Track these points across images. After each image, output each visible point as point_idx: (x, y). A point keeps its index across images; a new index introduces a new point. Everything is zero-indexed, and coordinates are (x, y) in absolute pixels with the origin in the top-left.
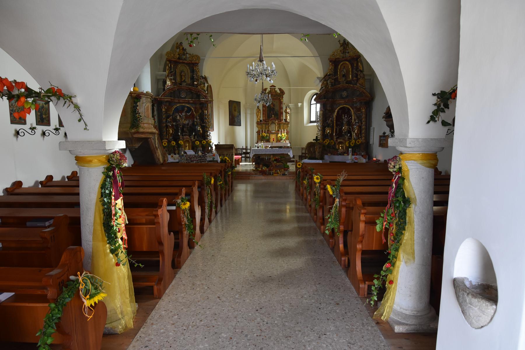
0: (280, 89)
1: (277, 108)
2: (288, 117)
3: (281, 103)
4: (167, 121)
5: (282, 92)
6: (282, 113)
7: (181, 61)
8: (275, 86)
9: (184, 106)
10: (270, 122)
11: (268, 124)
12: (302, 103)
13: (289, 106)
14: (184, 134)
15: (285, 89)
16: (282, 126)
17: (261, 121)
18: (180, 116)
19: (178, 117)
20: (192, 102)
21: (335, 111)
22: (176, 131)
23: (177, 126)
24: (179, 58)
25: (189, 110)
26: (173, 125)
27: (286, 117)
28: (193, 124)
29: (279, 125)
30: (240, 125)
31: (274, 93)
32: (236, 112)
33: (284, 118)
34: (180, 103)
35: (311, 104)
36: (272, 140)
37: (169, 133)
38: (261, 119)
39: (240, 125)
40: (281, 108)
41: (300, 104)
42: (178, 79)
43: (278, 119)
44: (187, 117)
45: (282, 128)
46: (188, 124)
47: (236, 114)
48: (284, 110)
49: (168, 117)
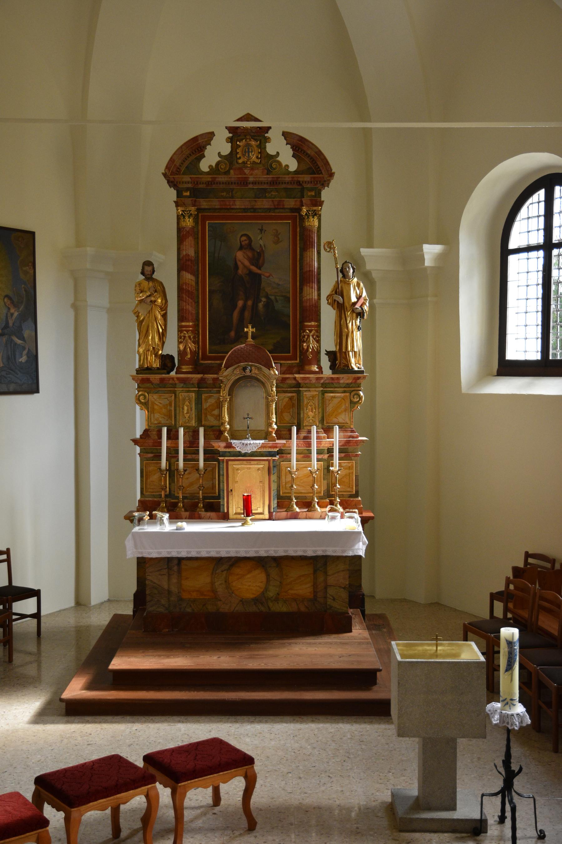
1: (277, 277)
2: (357, 341)
3: (304, 240)
5: (315, 167)
6: (314, 313)
10: (228, 375)
11: (217, 385)
12: (449, 239)
13: (358, 264)
15: (330, 137)
16: (310, 395)
17: (167, 362)
27: (342, 335)
29: (293, 390)
30: (32, 387)
31: (259, 175)
33: (328, 342)
35: (506, 252)
36: (235, 506)
38: (171, 348)
40: (307, 277)
41: (431, 251)
45: (310, 414)
48: (327, 284)
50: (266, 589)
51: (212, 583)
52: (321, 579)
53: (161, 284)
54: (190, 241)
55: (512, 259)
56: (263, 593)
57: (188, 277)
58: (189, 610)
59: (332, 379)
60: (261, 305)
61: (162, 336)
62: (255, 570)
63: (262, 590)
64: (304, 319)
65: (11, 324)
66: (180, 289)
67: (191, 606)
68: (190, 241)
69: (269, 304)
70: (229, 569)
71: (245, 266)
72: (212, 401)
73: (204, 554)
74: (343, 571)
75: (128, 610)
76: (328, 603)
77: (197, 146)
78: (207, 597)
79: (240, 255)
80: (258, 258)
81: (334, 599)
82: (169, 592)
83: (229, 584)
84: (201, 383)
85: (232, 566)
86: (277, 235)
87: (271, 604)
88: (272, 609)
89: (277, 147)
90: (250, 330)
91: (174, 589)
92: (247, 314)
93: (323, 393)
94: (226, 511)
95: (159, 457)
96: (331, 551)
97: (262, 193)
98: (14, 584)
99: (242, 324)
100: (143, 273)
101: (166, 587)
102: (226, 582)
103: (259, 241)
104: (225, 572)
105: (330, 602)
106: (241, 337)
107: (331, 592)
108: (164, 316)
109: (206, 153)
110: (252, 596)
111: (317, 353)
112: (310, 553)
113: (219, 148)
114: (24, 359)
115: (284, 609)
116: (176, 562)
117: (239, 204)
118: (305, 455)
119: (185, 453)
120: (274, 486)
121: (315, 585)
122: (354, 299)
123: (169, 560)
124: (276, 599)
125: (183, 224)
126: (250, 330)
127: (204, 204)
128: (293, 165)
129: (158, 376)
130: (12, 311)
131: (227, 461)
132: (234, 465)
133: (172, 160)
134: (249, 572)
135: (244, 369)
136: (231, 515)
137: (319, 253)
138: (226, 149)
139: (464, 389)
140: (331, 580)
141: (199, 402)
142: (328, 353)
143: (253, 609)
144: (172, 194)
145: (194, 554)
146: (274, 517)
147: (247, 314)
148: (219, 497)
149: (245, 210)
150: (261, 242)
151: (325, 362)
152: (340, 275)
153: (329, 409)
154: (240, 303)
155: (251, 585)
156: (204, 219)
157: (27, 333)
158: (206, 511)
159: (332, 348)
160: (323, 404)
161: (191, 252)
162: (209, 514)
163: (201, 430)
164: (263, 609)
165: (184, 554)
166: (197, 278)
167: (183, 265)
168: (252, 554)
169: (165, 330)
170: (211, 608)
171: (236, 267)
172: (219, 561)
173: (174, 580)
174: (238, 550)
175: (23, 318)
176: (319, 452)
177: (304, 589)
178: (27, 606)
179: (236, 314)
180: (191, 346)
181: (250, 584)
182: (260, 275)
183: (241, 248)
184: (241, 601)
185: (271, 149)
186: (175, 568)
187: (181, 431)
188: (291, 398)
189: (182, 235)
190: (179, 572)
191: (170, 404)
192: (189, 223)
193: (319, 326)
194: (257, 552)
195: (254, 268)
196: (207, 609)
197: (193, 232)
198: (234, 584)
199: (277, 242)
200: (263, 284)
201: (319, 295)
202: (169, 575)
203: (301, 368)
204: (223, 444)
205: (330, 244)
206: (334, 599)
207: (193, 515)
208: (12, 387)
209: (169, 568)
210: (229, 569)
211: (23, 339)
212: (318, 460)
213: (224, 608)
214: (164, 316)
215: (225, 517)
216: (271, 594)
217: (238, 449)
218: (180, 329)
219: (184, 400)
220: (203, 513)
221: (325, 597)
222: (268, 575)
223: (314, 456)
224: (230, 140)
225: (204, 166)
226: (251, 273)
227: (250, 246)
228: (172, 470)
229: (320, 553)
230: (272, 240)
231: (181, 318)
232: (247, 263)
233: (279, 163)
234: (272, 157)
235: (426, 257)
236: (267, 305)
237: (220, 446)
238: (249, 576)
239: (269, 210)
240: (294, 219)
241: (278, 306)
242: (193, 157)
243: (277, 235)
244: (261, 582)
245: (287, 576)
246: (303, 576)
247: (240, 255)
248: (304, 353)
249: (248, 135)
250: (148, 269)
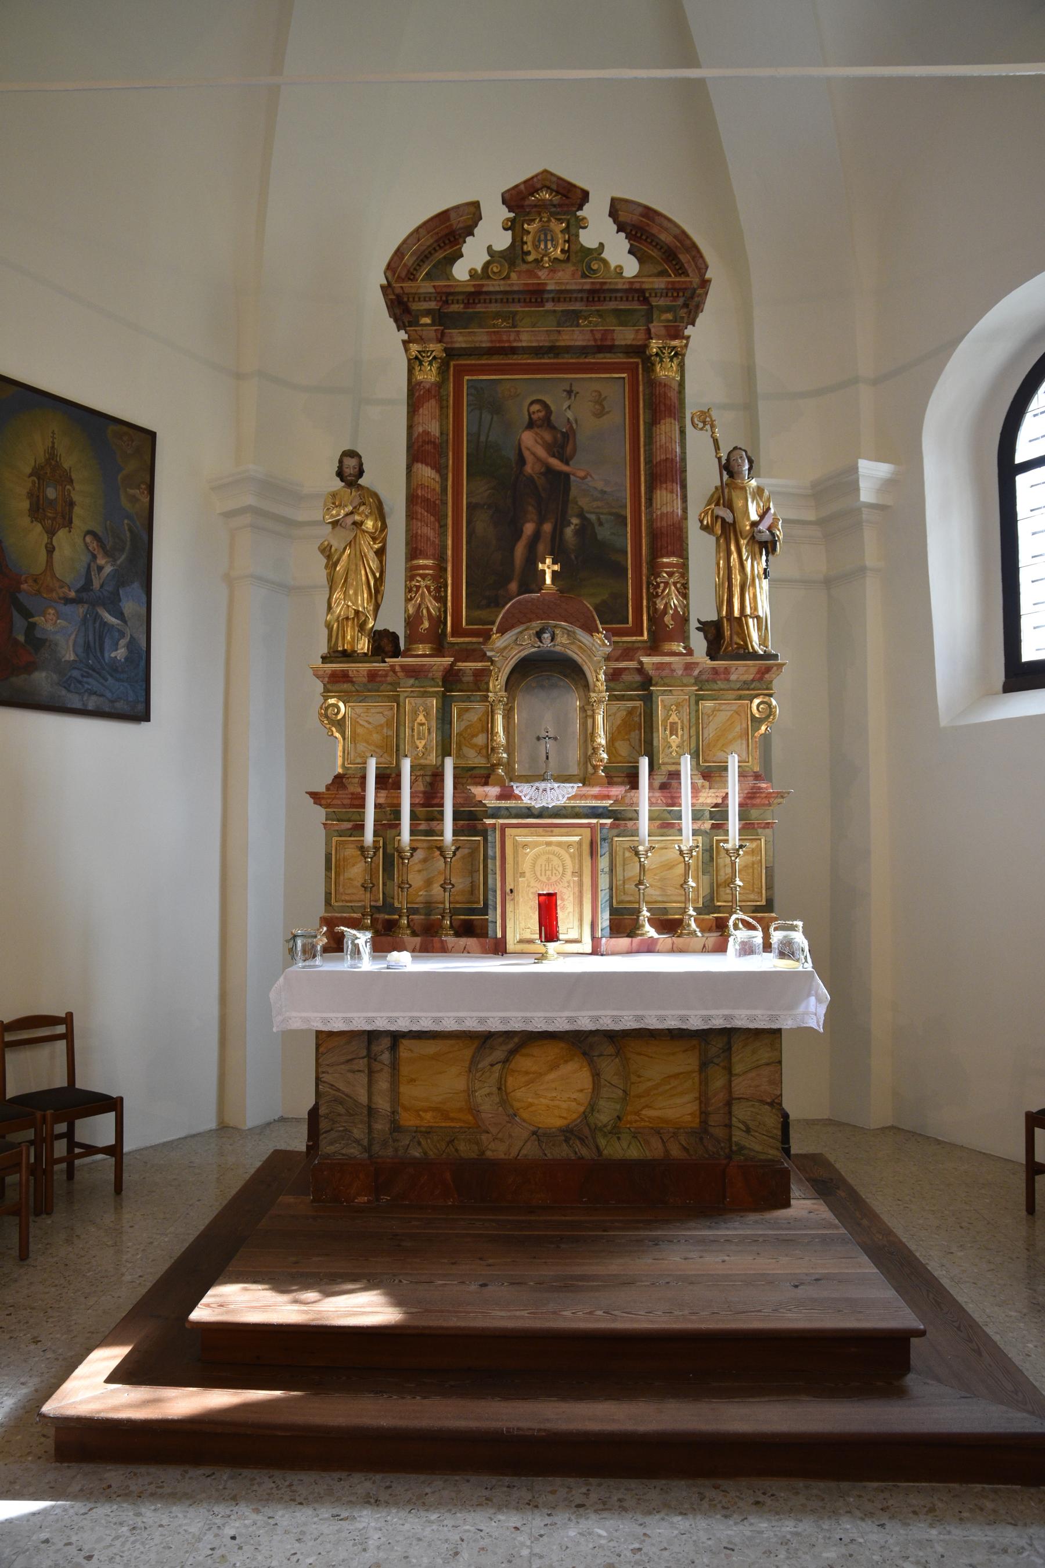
0: (638, 225)
1: (601, 476)
11: (481, 678)
12: (906, 453)
16: (669, 707)
17: (384, 644)
29: (639, 690)
30: (138, 712)
31: (566, 278)
32: (70, 550)
35: (1008, 470)
36: (521, 922)
38: (392, 618)
41: (872, 474)
43: (612, 615)
45: (670, 741)
50: (592, 1107)
51: (470, 1092)
52: (718, 1083)
53: (375, 495)
54: (429, 408)
55: (1022, 481)
56: (585, 1116)
57: (426, 473)
58: (417, 1153)
59: (715, 671)
60: (569, 532)
61: (376, 594)
62: (566, 1062)
63: (582, 1109)
64: (655, 553)
65: (96, 584)
66: (412, 499)
67: (419, 1143)
68: (429, 408)
69: (585, 530)
70: (506, 1061)
71: (538, 459)
72: (473, 717)
73: (449, 1025)
74: (767, 1064)
75: (299, 1143)
76: (734, 1139)
77: (449, 230)
78: (458, 1125)
79: (528, 438)
80: (563, 444)
81: (748, 1130)
82: (371, 1111)
83: (507, 1094)
84: (451, 679)
85: (513, 1052)
87: (602, 1142)
88: (605, 1152)
89: (599, 231)
90: (548, 568)
91: (383, 1104)
93: (699, 698)
94: (499, 935)
95: (360, 828)
96: (744, 1017)
97: (572, 318)
98: (78, 1085)
99: (532, 559)
100: (340, 474)
101: (363, 1099)
102: (499, 1089)
103: (564, 411)
104: (499, 1066)
105: (738, 1136)
106: (532, 579)
107: (741, 1112)
108: (380, 553)
109: (465, 249)
110: (560, 1123)
111: (683, 620)
112: (695, 1023)
113: (492, 235)
114: (120, 653)
115: (634, 1152)
116: (386, 1042)
117: (526, 339)
118: (666, 823)
119: (414, 816)
120: (604, 882)
121: (703, 1099)
122: (754, 517)
123: (372, 1036)
124: (614, 1131)
125: (420, 377)
127: (460, 339)
128: (631, 267)
129: (364, 667)
130: (101, 561)
131: (503, 827)
132: (517, 837)
133: (399, 253)
134: (554, 1067)
135: (539, 635)
136: (511, 946)
137: (683, 432)
138: (503, 241)
139: (944, 721)
140: (740, 1087)
141: (444, 718)
142: (704, 627)
143: (563, 1152)
145: (426, 1024)
146: (603, 949)
148: (484, 911)
149: (537, 351)
150: (569, 414)
151: (699, 642)
152: (726, 477)
153: (709, 732)
154: (529, 528)
155: (555, 1097)
156: (460, 371)
157: (129, 606)
158: (458, 934)
160: (696, 723)
161: (434, 428)
162: (463, 941)
163: (449, 763)
164: (584, 1152)
165: (403, 1025)
166: (444, 479)
167: (419, 451)
168: (561, 1025)
169: (380, 581)
170: (466, 1150)
171: (521, 460)
172: (484, 1040)
173: (383, 1084)
174: (528, 1014)
175: (121, 580)
176: (697, 816)
177: (678, 1107)
178: (98, 1130)
179: (520, 550)
180: (432, 605)
181: (554, 1094)
182: (567, 476)
183: (531, 425)
184: (534, 1133)
185: (588, 239)
186: (386, 1057)
187: (406, 765)
188: (631, 712)
189: (416, 396)
190: (395, 1066)
191: (389, 724)
192: (429, 375)
193: (684, 567)
194: (571, 1020)
195: (555, 463)
196: (457, 1150)
197: (436, 392)
198: (518, 1094)
199: (600, 414)
200: (574, 492)
201: (685, 510)
202: (371, 1073)
203: (654, 647)
204: (493, 791)
205: (705, 419)
206: (748, 1130)
207: (429, 938)
208: (92, 703)
209: (371, 1058)
210: (506, 1061)
211: (121, 616)
212: (695, 833)
213: (497, 1151)
214: (380, 553)
215: (499, 948)
216: (604, 1117)
217: (526, 800)
218: (411, 573)
219: (415, 713)
220: (450, 940)
221: (729, 1126)
222: (596, 1075)
223: (687, 823)
224: (510, 226)
225: (461, 271)
226: (549, 471)
227: (547, 421)
228: (390, 857)
229: (718, 1023)
230: (593, 408)
231: (413, 552)
232: (541, 452)
233: (605, 262)
234: (589, 251)
235: (863, 484)
236: (580, 532)
237: (488, 794)
238: (552, 1076)
239: (584, 351)
240: (632, 370)
241: (604, 533)
242: (440, 255)
243: (600, 401)
244: (581, 1091)
245: (639, 1076)
246: (676, 1076)
247: (528, 438)
248: (656, 619)
249: (546, 201)
250: (350, 463)
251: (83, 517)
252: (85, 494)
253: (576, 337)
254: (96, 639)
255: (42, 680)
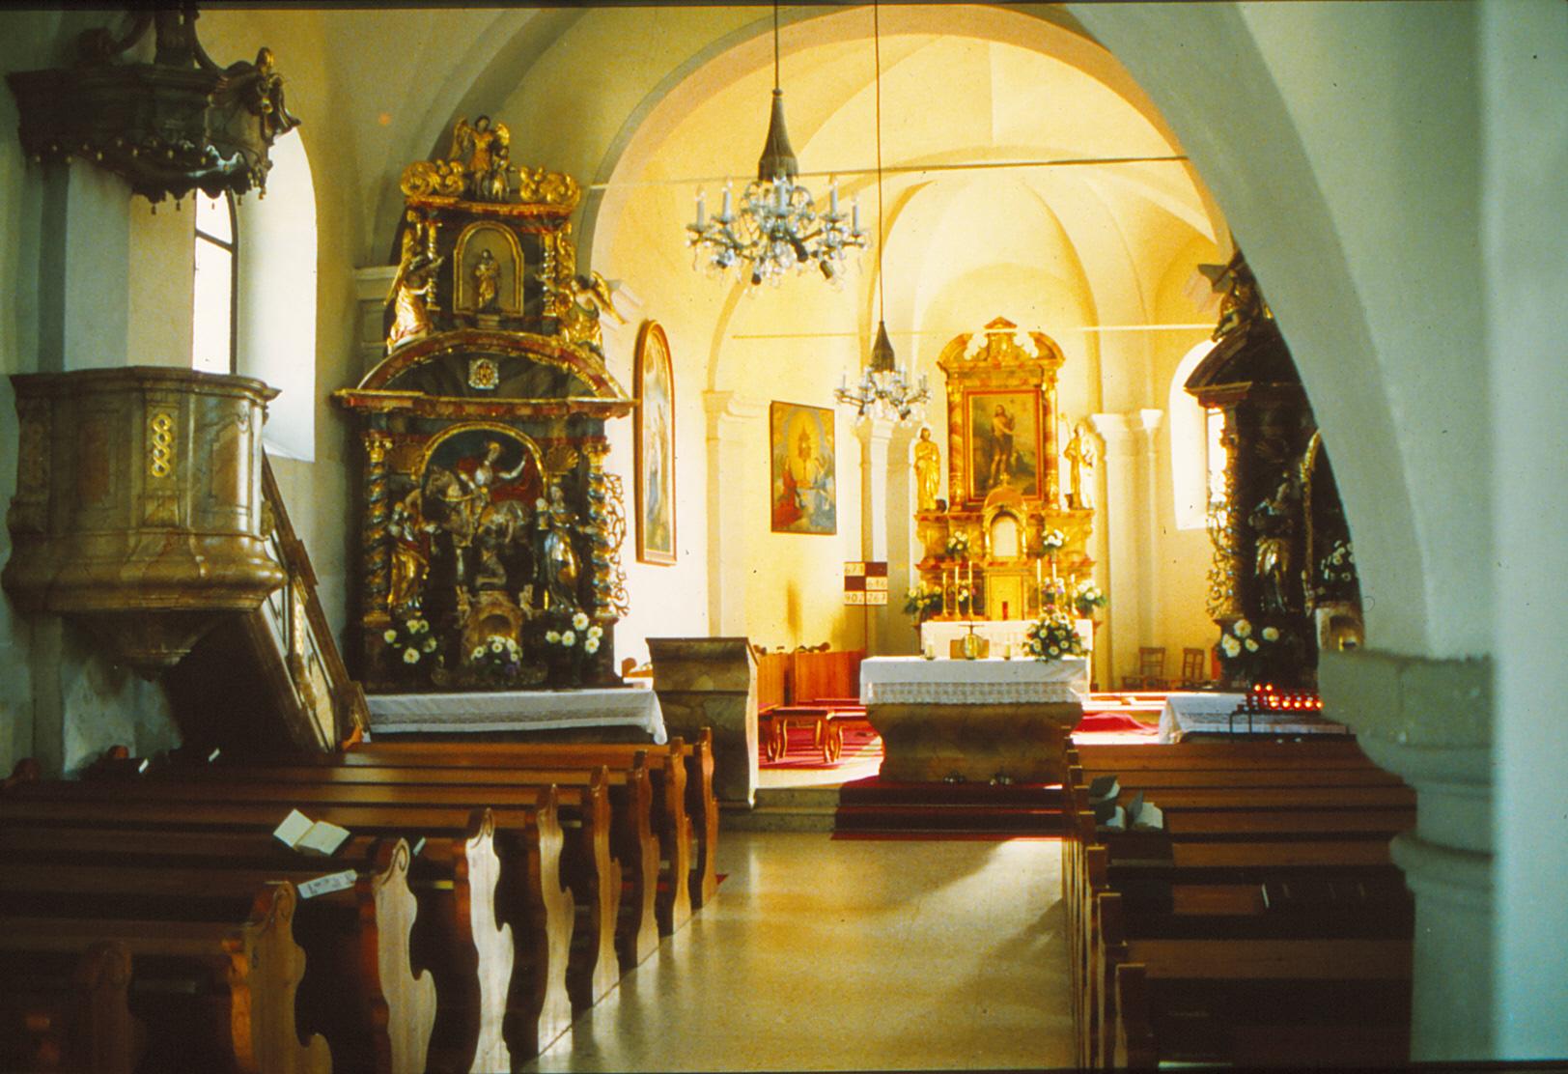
0: (1039, 339)
1: (1024, 437)
4: (390, 511)
7: (477, 208)
8: (1009, 324)
9: (490, 436)
14: (480, 580)
18: (464, 488)
19: (453, 493)
20: (526, 412)
21: (1306, 446)
22: (440, 565)
23: (444, 539)
24: (470, 195)
25: (512, 452)
26: (422, 538)
27: (1075, 480)
28: (530, 528)
32: (811, 465)
34: (465, 420)
36: (994, 607)
37: (402, 578)
39: (831, 531)
40: (1045, 437)
42: (461, 298)
44: (500, 492)
46: (502, 531)
47: (807, 470)
49: (394, 495)
60: (1013, 460)
69: (1019, 458)
77: (962, 341)
80: (1009, 424)
86: (1024, 404)
92: (1002, 466)
97: (1012, 373)
103: (1010, 410)
111: (1057, 495)
126: (1004, 477)
128: (1035, 353)
138: (984, 342)
144: (944, 375)
147: (1002, 466)
151: (1064, 502)
157: (829, 487)
159: (1070, 491)
167: (952, 430)
175: (826, 475)
185: (1017, 341)
192: (957, 398)
225: (968, 355)
251: (814, 454)
252: (813, 442)
253: (1014, 382)
254: (820, 500)
255: (804, 521)
